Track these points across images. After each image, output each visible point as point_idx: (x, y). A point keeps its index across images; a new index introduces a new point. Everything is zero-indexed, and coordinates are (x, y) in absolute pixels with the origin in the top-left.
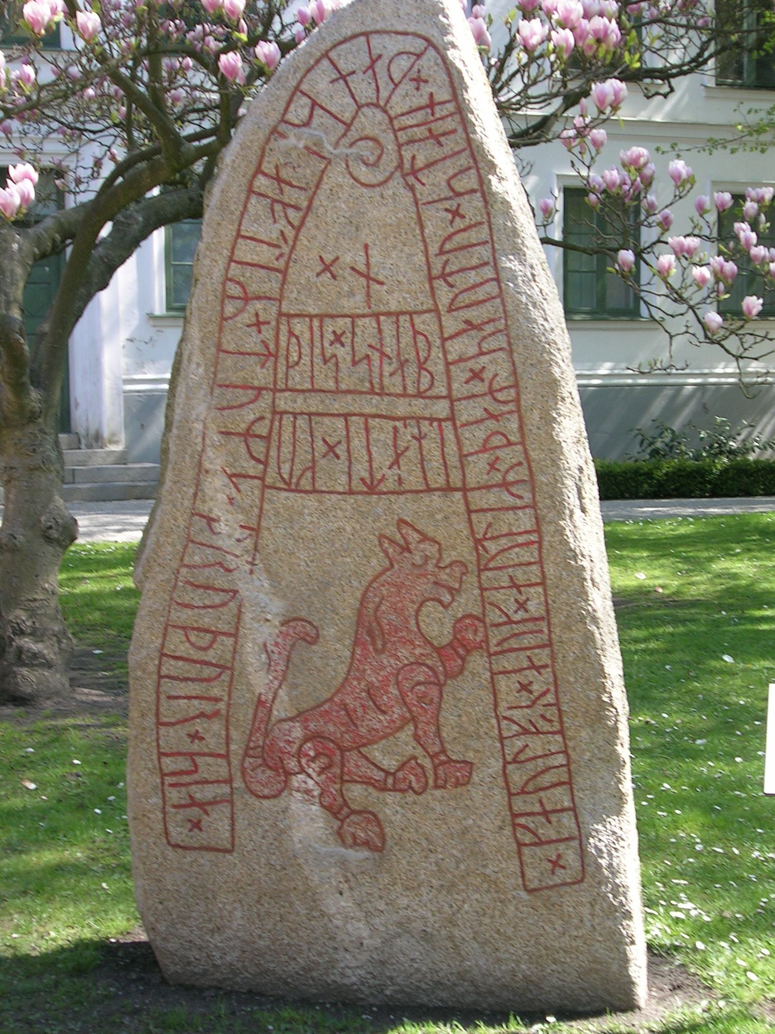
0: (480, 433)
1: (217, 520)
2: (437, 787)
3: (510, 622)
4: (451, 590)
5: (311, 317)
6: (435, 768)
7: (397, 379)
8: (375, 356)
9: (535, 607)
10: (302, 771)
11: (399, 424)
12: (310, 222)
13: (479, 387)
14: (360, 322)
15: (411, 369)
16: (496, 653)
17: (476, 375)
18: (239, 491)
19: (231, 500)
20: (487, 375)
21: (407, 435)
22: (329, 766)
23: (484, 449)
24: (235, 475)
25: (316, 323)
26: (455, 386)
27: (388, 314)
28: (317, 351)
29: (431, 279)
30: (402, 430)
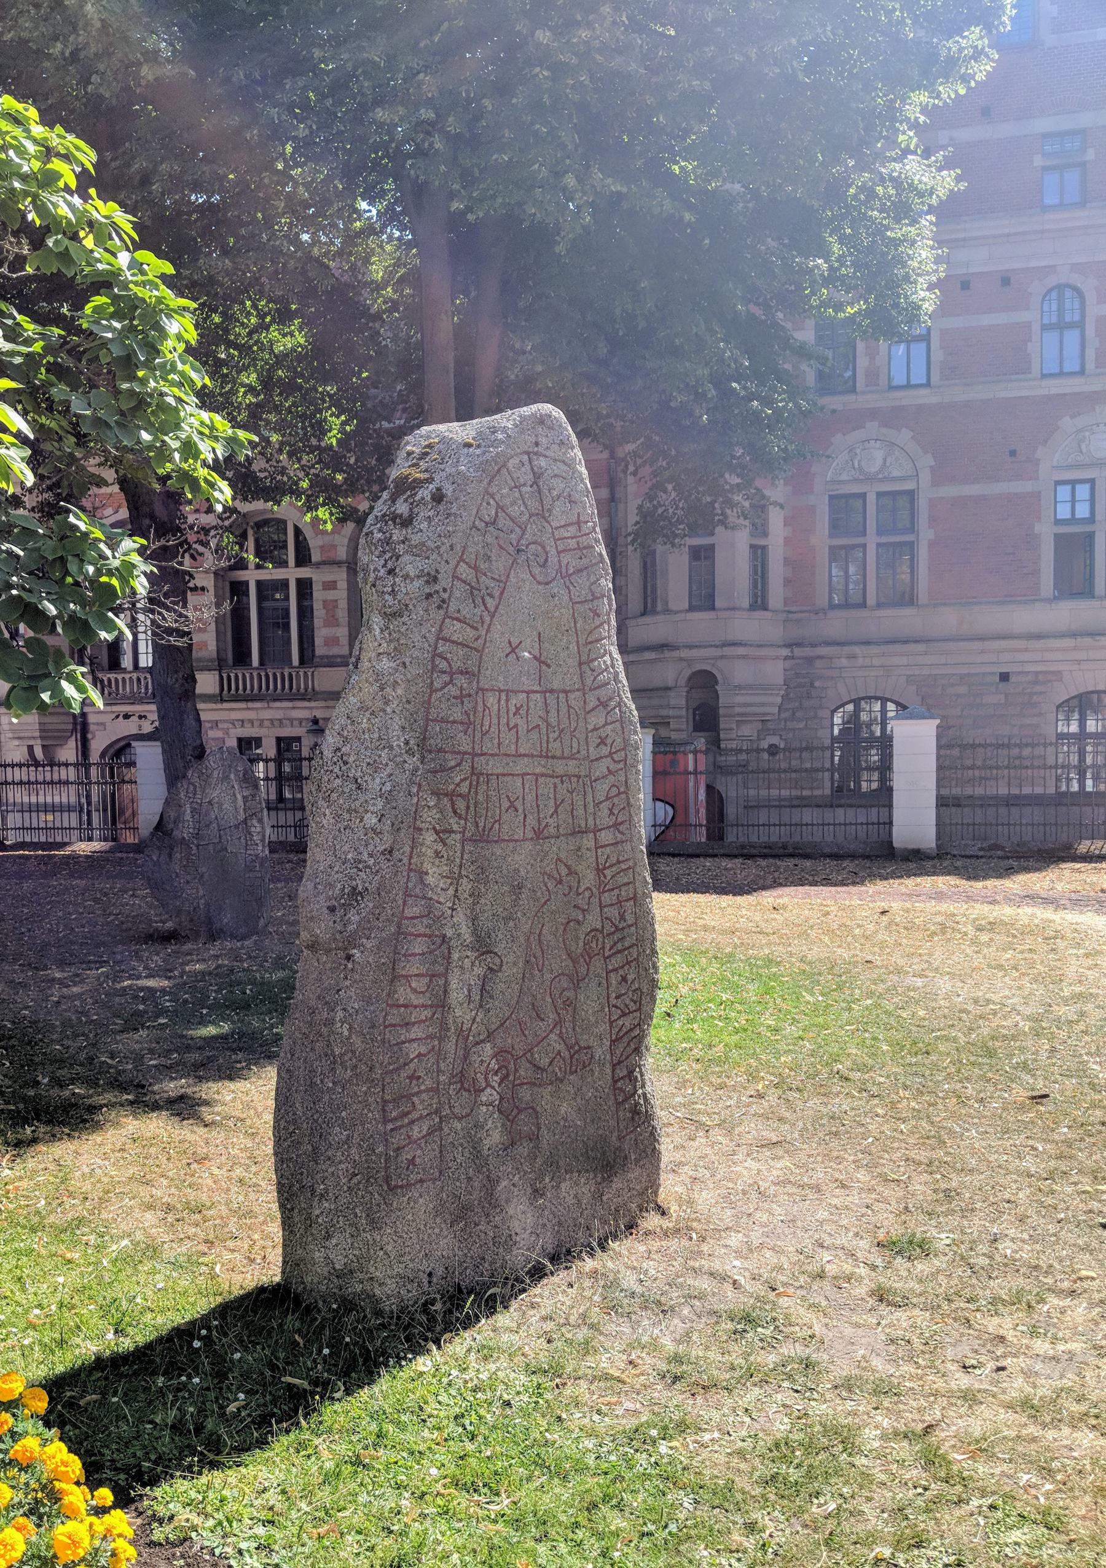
0: (606, 787)
1: (427, 873)
2: (572, 1073)
3: (617, 929)
4: (583, 910)
5: (500, 691)
6: (572, 1057)
7: (557, 745)
8: (543, 726)
9: (630, 919)
10: (488, 1085)
11: (558, 781)
12: (501, 610)
13: (605, 751)
14: (533, 696)
15: (567, 737)
16: (609, 957)
17: (602, 742)
18: (445, 844)
19: (437, 854)
20: (609, 741)
21: (562, 790)
22: (507, 1076)
23: (607, 799)
24: (443, 831)
25: (504, 697)
26: (591, 749)
27: (552, 691)
28: (504, 721)
29: (580, 664)
30: (559, 786)
